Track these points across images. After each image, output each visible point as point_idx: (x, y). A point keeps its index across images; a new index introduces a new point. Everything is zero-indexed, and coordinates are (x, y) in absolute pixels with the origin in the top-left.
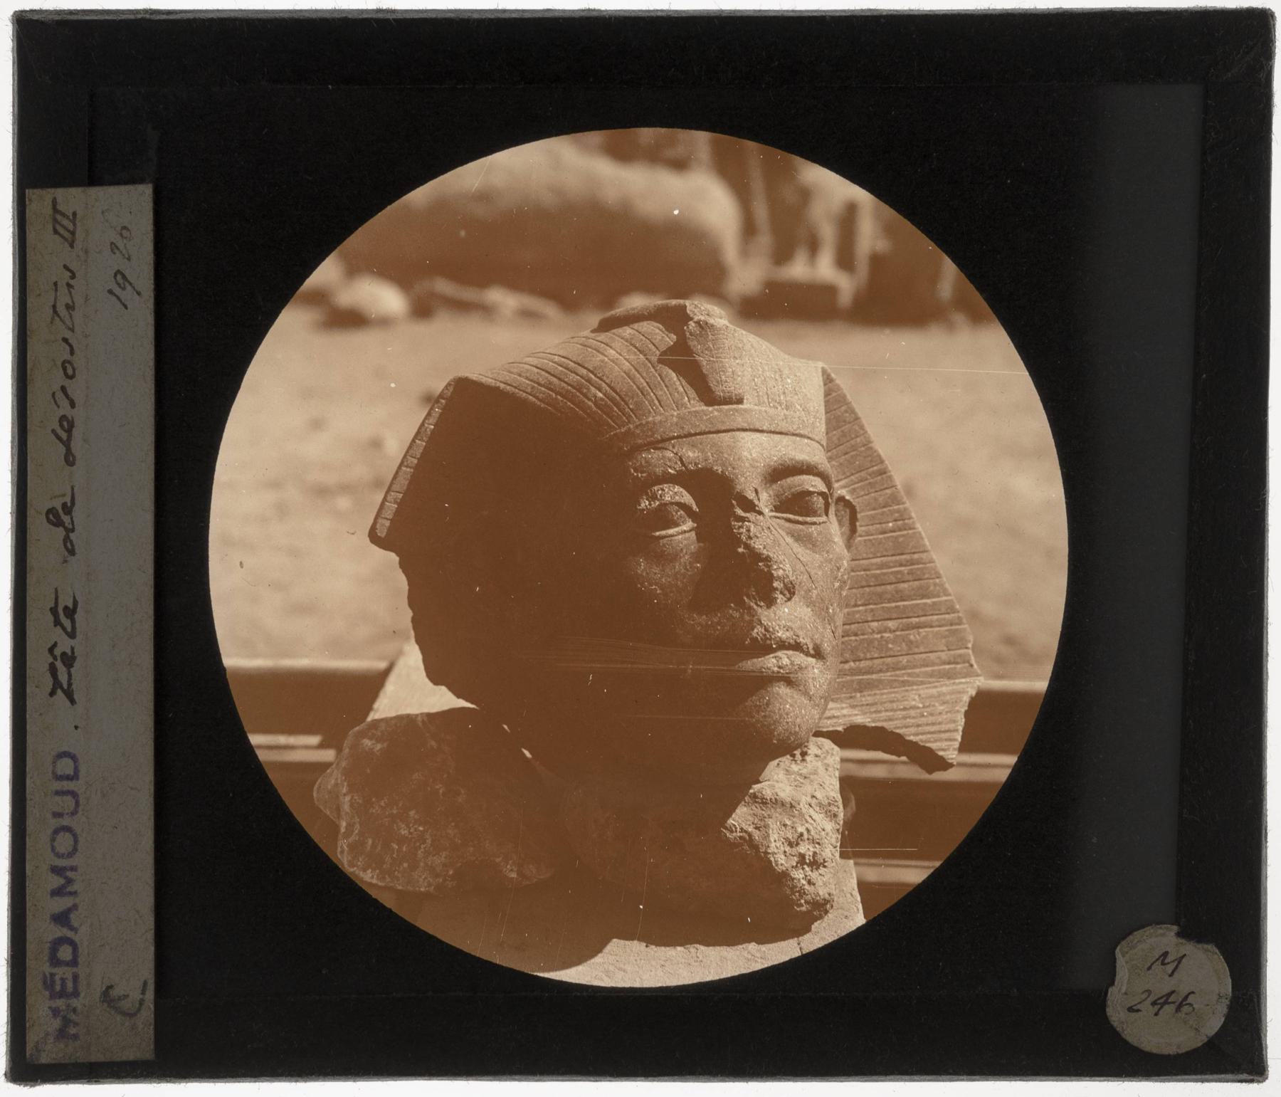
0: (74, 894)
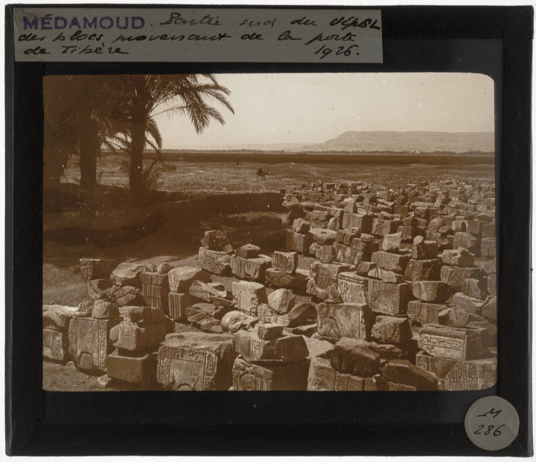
0: (85, 27)
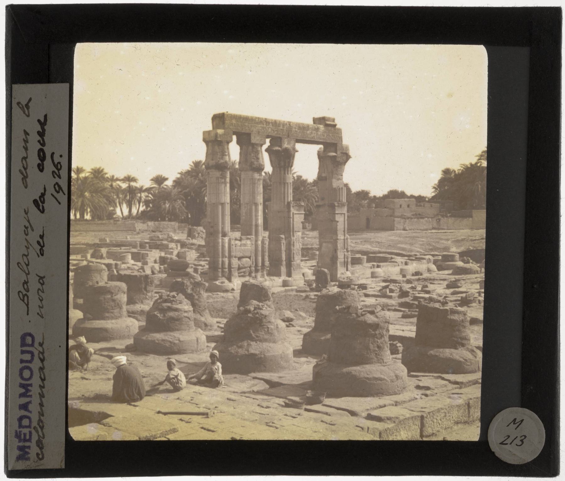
0: (31, 396)
